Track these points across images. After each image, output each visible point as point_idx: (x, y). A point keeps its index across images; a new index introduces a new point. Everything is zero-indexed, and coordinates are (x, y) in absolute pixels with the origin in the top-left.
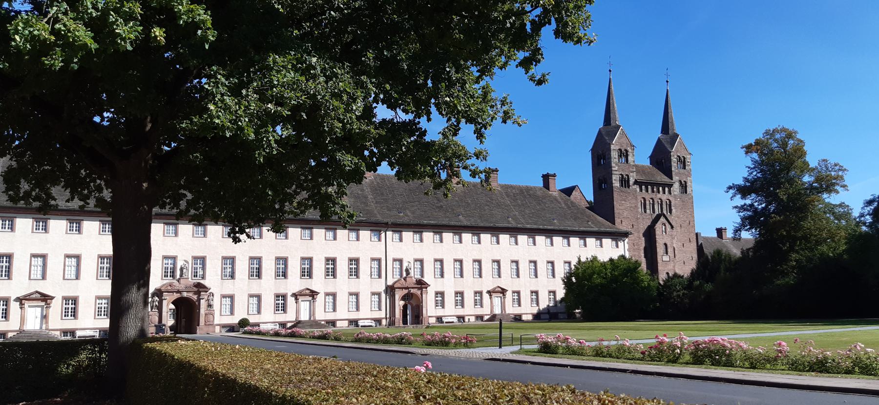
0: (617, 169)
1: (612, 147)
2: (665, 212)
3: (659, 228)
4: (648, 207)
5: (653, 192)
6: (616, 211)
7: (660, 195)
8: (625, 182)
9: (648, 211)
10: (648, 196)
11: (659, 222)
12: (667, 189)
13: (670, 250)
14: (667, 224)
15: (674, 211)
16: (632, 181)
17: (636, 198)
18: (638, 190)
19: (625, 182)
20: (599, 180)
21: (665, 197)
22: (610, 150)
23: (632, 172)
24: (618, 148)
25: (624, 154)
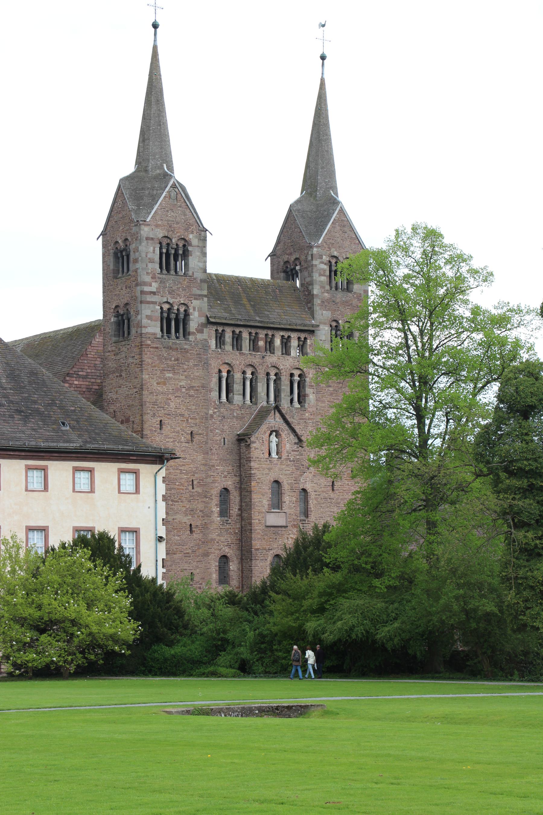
0: (154, 292)
1: (145, 231)
2: (285, 404)
3: (262, 444)
4: (237, 387)
5: (254, 347)
6: (147, 397)
7: (271, 359)
8: (174, 322)
9: (237, 399)
10: (239, 360)
11: (264, 428)
12: (294, 343)
13: (290, 499)
14: (285, 432)
15: (311, 397)
16: (195, 320)
17: (206, 365)
18: (213, 343)
19: (174, 322)
20: (118, 315)
21: (289, 363)
22: (137, 237)
23: (199, 297)
24: (160, 233)
25: (176, 254)
